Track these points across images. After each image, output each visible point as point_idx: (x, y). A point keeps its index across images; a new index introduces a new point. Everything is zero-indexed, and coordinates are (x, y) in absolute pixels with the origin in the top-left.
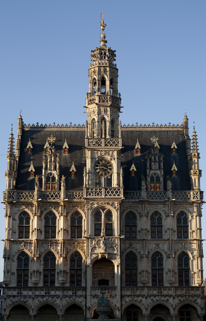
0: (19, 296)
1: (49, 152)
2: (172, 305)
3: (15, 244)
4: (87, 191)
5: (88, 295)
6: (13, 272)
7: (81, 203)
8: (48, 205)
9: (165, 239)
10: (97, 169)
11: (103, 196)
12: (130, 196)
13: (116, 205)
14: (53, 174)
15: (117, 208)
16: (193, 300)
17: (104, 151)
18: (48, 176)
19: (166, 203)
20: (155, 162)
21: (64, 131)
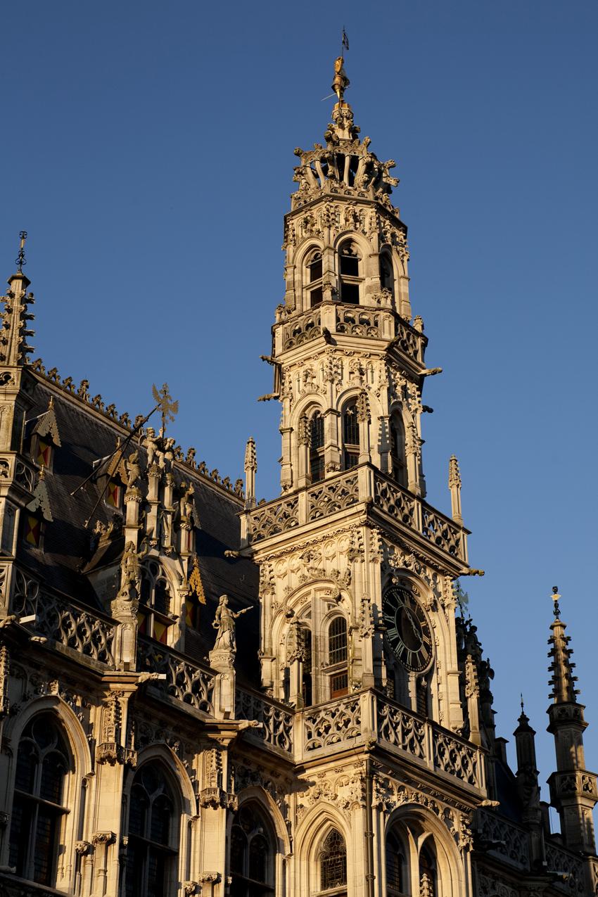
7: (280, 770)
8: (154, 724)
13: (457, 826)
14: (164, 574)
15: (462, 844)
19: (524, 883)
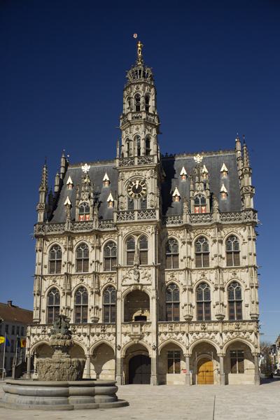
2: (218, 344)
9: (213, 267)
10: (130, 191)
11: (136, 220)
16: (245, 336)
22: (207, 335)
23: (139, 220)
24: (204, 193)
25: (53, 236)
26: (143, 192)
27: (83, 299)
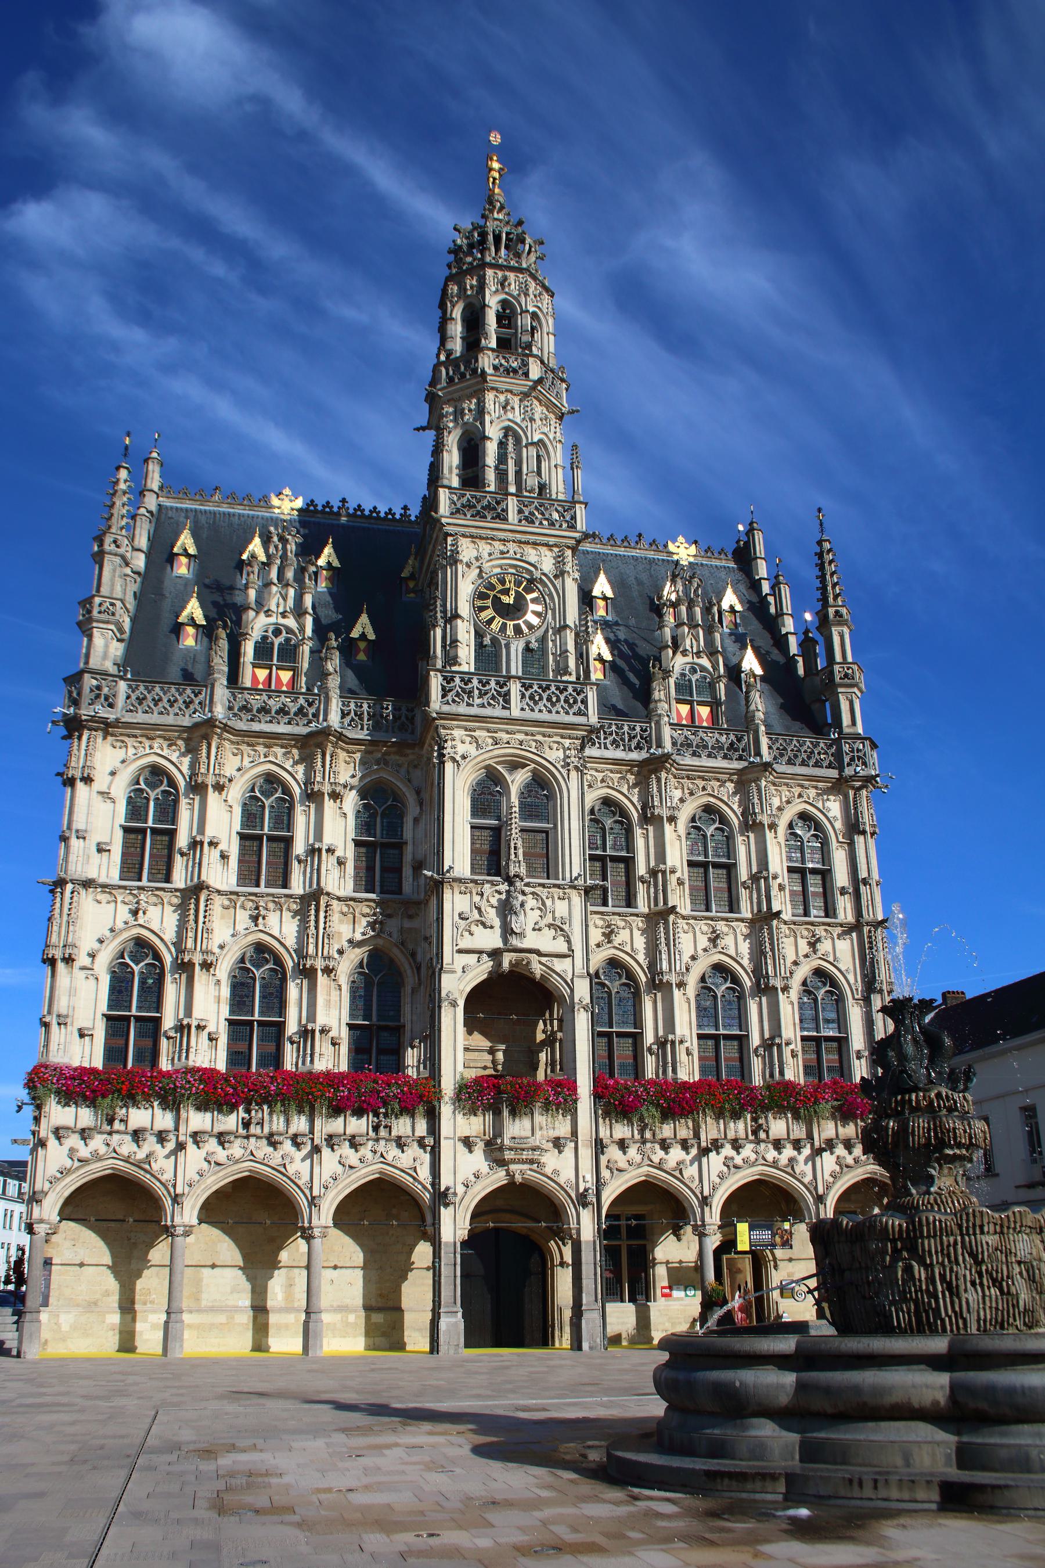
0: (110, 1133)
1: (276, 547)
3: (104, 904)
4: (443, 688)
5: (446, 1138)
6: (85, 1023)
10: (482, 609)
11: (515, 712)
12: (605, 738)
17: (514, 541)
18: (264, 638)
20: (693, 626)
21: (319, 523)
22: (771, 1154)
23: (528, 715)
24: (705, 662)
25: (149, 731)
26: (530, 617)
27: (263, 997)
